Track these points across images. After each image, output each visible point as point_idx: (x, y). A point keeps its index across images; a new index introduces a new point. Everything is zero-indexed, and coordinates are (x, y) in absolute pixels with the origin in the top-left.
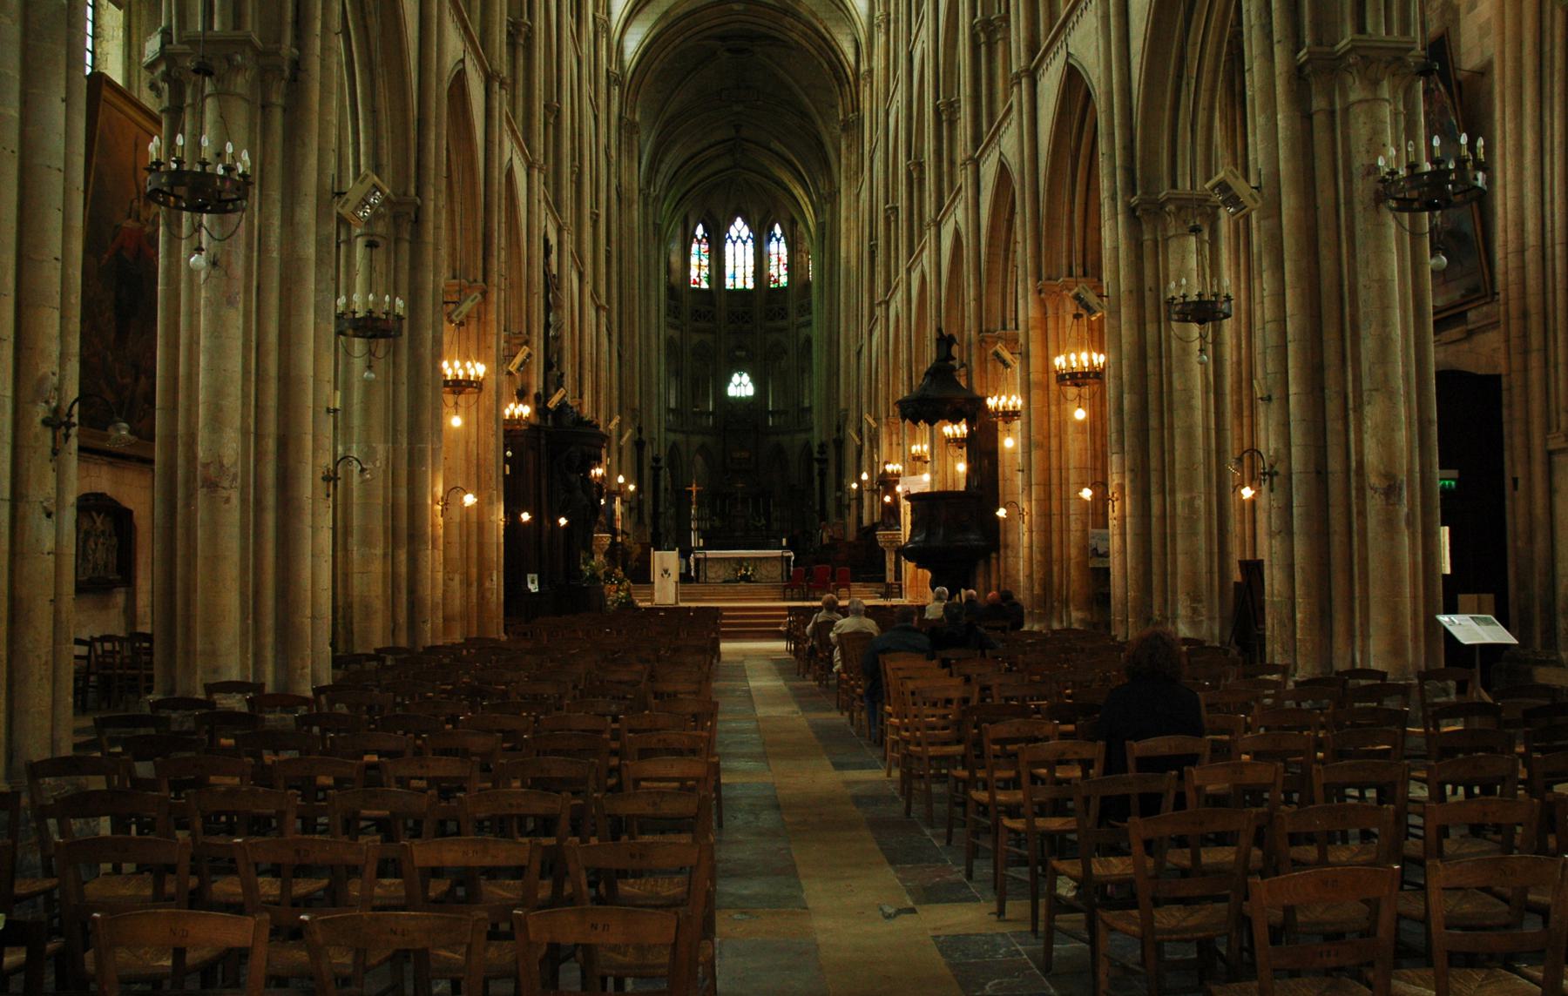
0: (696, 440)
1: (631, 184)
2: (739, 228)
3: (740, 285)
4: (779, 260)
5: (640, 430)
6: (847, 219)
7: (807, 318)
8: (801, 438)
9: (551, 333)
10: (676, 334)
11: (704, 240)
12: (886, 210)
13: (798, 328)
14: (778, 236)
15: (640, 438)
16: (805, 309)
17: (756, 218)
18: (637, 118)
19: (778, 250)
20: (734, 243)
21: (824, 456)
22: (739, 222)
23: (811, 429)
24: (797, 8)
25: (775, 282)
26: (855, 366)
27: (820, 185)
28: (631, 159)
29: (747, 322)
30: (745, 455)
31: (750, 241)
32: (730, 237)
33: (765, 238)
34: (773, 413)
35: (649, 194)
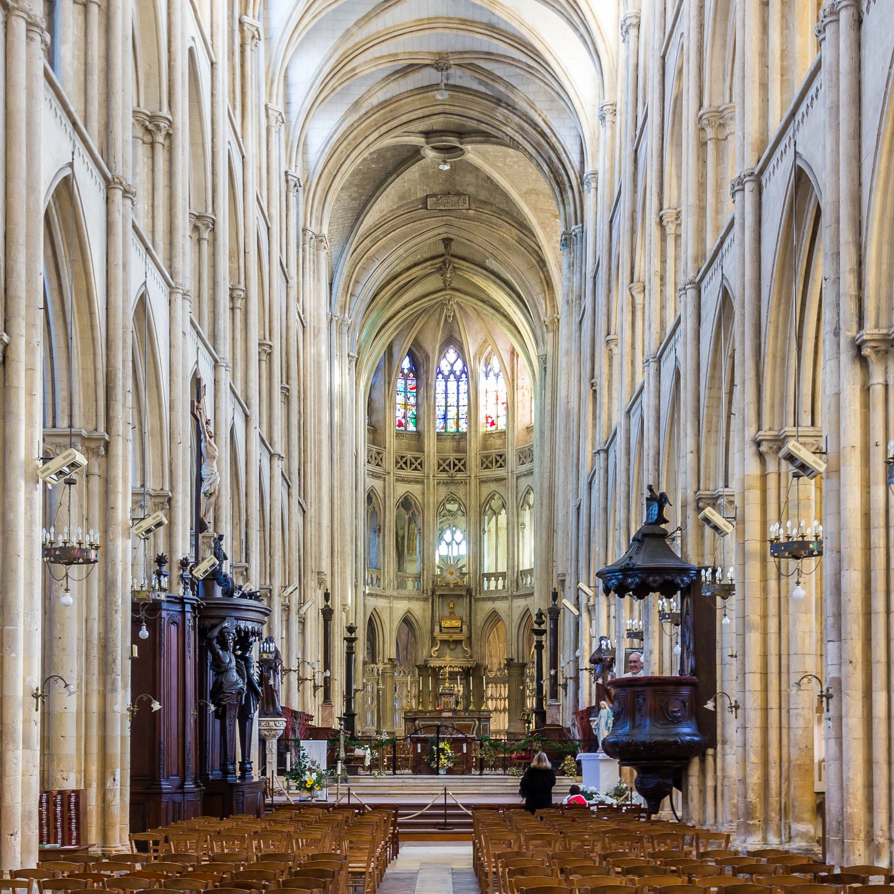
0: (401, 607)
1: (317, 308)
5: (327, 596)
6: (568, 352)
8: (520, 604)
9: (205, 487)
10: (378, 484)
11: (411, 375)
15: (327, 606)
18: (325, 231)
20: (446, 379)
23: (532, 594)
24: (512, 96)
26: (574, 524)
27: (542, 312)
29: (460, 470)
30: (456, 623)
32: (440, 372)
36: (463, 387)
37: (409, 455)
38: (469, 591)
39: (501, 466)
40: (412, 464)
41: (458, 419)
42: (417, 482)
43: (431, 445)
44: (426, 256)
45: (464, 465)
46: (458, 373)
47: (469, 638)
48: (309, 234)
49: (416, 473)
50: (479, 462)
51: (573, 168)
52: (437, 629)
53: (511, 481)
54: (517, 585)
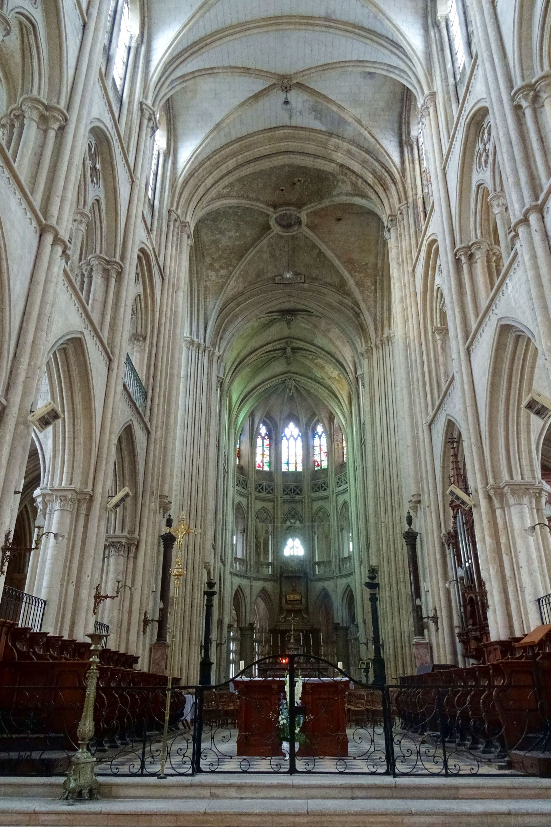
0: (258, 585)
3: (292, 469)
4: (321, 450)
7: (344, 487)
10: (244, 501)
11: (266, 437)
12: (512, 99)
13: (337, 496)
14: (320, 434)
16: (341, 480)
17: (304, 419)
20: (288, 439)
21: (376, 581)
22: (292, 425)
25: (318, 465)
26: (427, 440)
27: (358, 346)
28: (179, 246)
29: (298, 494)
30: (297, 597)
31: (299, 438)
32: (285, 436)
33: (310, 434)
34: (318, 563)
35: (214, 353)
37: (264, 483)
38: (306, 574)
39: (325, 489)
40: (266, 489)
41: (296, 464)
42: (269, 501)
43: (279, 480)
44: (275, 338)
45: (301, 490)
46: (296, 437)
47: (307, 608)
48: (174, 216)
49: (269, 495)
50: (310, 488)
51: (395, 166)
52: (284, 601)
53: (333, 498)
54: (340, 569)
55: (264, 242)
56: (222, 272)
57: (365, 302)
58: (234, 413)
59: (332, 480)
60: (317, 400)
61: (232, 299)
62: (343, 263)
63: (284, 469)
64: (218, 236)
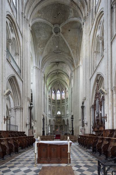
2: (58, 92)
3: (59, 99)
10: (50, 105)
19: (63, 94)
22: (58, 91)
36: (60, 94)
43: (56, 101)
55: (51, 39)
56: (42, 48)
57: (74, 57)
58: (48, 87)
59: (65, 101)
60: (63, 85)
61: (45, 57)
62: (70, 46)
63: (57, 99)
64: (40, 36)
